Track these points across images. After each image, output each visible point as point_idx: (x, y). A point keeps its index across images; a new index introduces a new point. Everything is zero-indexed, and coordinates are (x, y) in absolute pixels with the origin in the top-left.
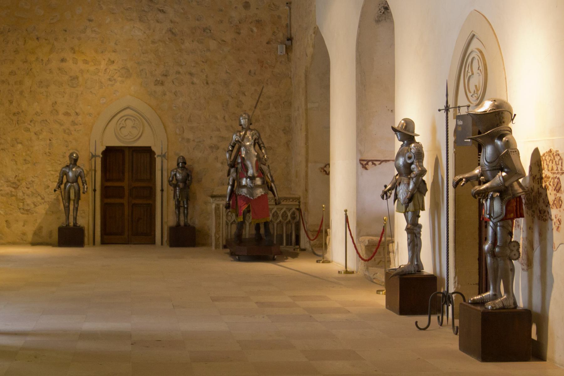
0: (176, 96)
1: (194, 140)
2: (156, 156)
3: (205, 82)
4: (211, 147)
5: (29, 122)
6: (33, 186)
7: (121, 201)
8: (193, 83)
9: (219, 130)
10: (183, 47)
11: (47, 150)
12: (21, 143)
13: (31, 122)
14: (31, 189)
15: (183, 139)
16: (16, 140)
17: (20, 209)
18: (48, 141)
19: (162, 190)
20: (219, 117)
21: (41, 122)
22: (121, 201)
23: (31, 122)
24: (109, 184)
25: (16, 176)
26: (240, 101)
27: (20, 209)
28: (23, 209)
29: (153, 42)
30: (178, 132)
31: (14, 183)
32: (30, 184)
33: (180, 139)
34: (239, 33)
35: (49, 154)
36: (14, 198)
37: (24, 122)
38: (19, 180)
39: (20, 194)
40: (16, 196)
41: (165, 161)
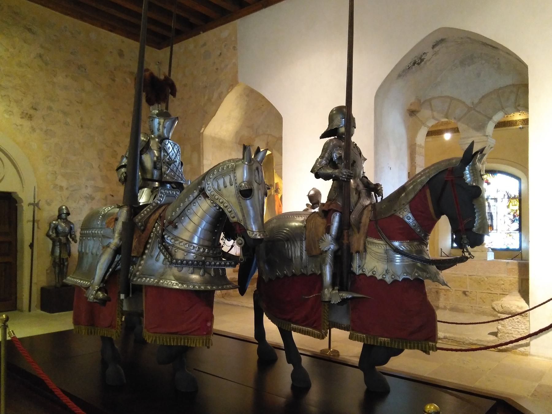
1: (67, 189)
3: (80, 125)
8: (67, 124)
9: (94, 179)
10: (55, 80)
20: (94, 165)
26: (115, 151)
29: (20, 65)
34: (114, 80)
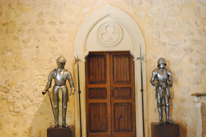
0: (152, 4)
1: (169, 44)
2: (135, 59)
4: (186, 50)
5: (17, 32)
6: (22, 90)
7: (104, 101)
9: (192, 34)
11: (35, 57)
12: (11, 51)
13: (19, 31)
14: (21, 93)
15: (159, 42)
16: (6, 48)
17: (10, 111)
18: (36, 48)
19: (142, 90)
20: (191, 22)
21: (28, 31)
22: (104, 101)
23: (19, 31)
24: (92, 86)
25: (7, 81)
27: (10, 111)
28: (14, 111)
30: (154, 36)
31: (4, 88)
32: (19, 88)
33: (157, 43)
35: (35, 60)
36: (5, 101)
37: (13, 32)
38: (9, 85)
39: (10, 98)
40: (7, 99)
41: (144, 64)
